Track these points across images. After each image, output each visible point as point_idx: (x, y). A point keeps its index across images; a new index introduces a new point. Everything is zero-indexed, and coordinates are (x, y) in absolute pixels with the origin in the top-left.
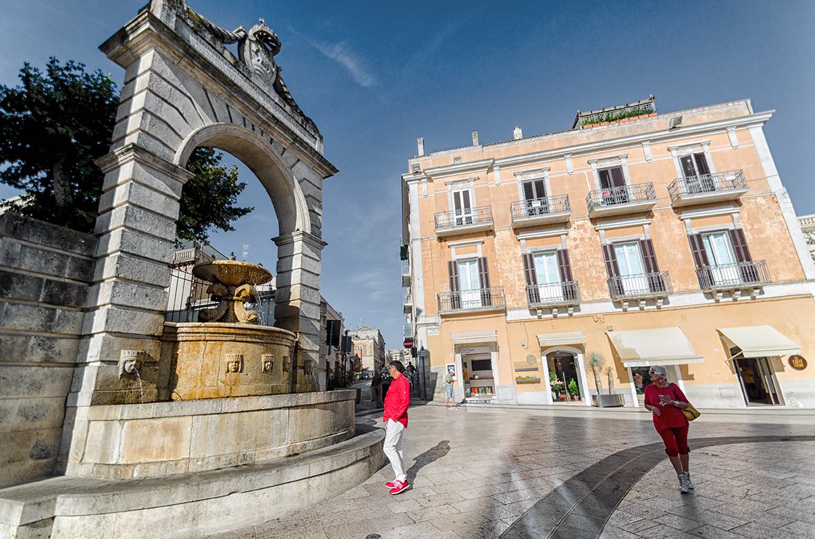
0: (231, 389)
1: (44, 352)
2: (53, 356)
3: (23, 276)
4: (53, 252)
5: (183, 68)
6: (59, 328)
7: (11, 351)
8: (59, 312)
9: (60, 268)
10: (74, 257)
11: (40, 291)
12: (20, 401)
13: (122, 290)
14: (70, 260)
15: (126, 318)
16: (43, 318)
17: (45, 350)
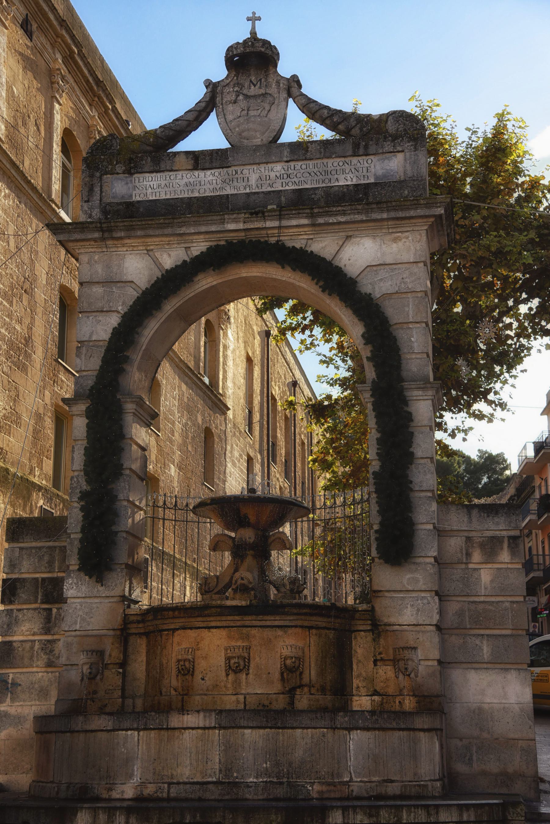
0: (183, 701)
1: (47, 657)
2: (54, 660)
3: (24, 579)
4: (43, 547)
5: (114, 250)
6: (56, 629)
7: (22, 658)
8: (54, 611)
9: (51, 563)
10: (60, 547)
11: (38, 592)
12: (34, 708)
13: (75, 581)
14: (57, 551)
15: (81, 613)
16: (42, 620)
17: (47, 654)
